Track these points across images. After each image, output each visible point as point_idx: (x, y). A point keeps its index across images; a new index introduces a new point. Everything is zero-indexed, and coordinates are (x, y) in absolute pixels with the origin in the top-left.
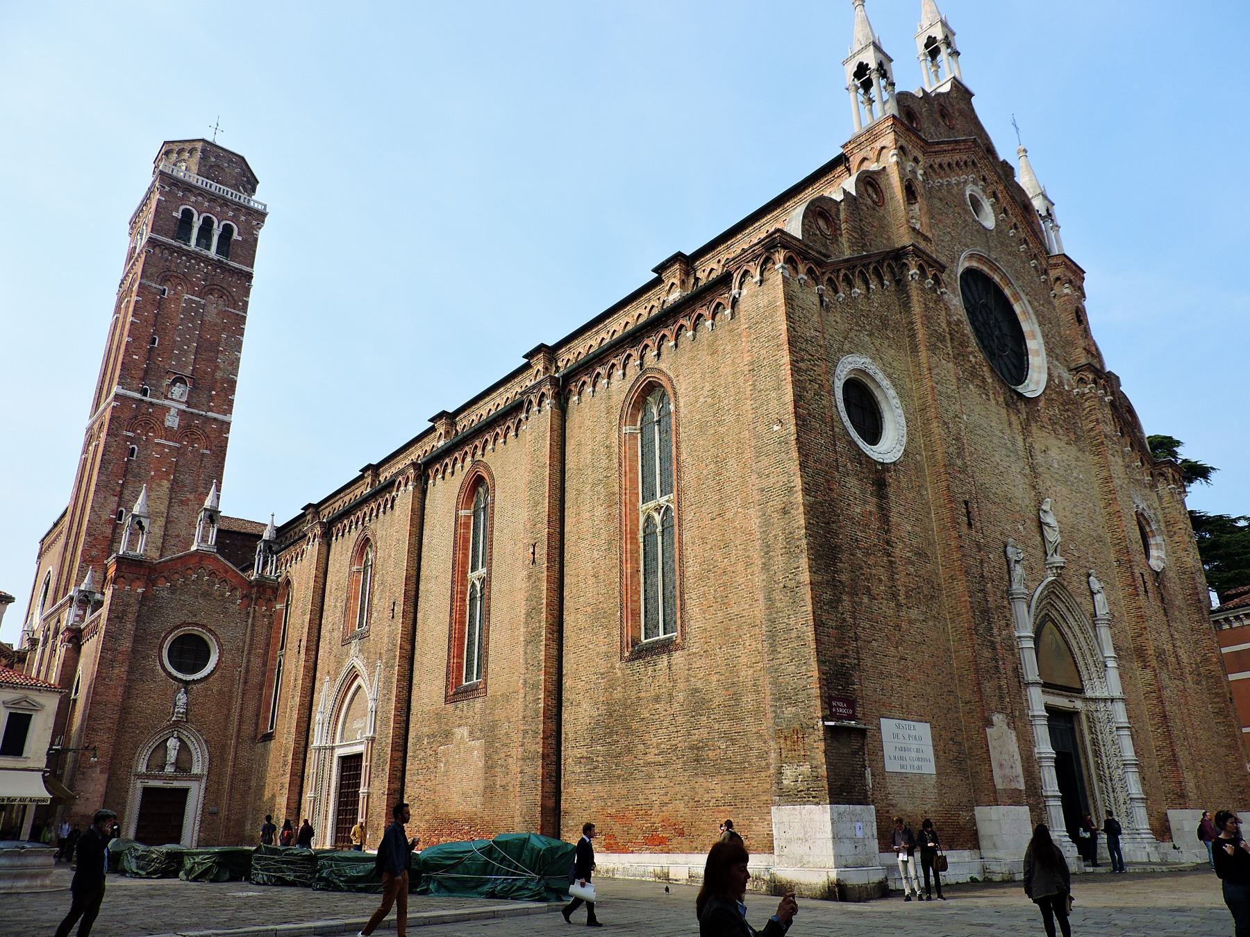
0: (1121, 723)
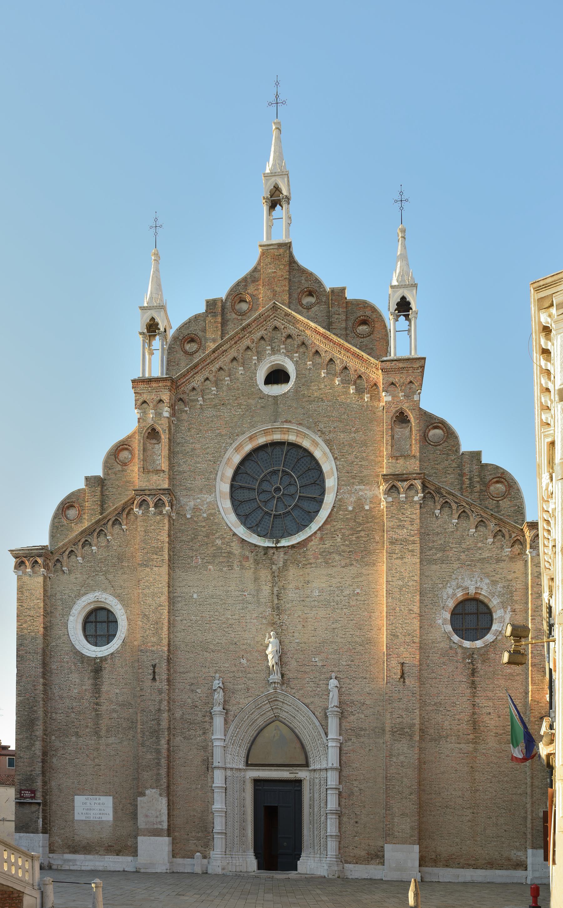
0: (329, 785)
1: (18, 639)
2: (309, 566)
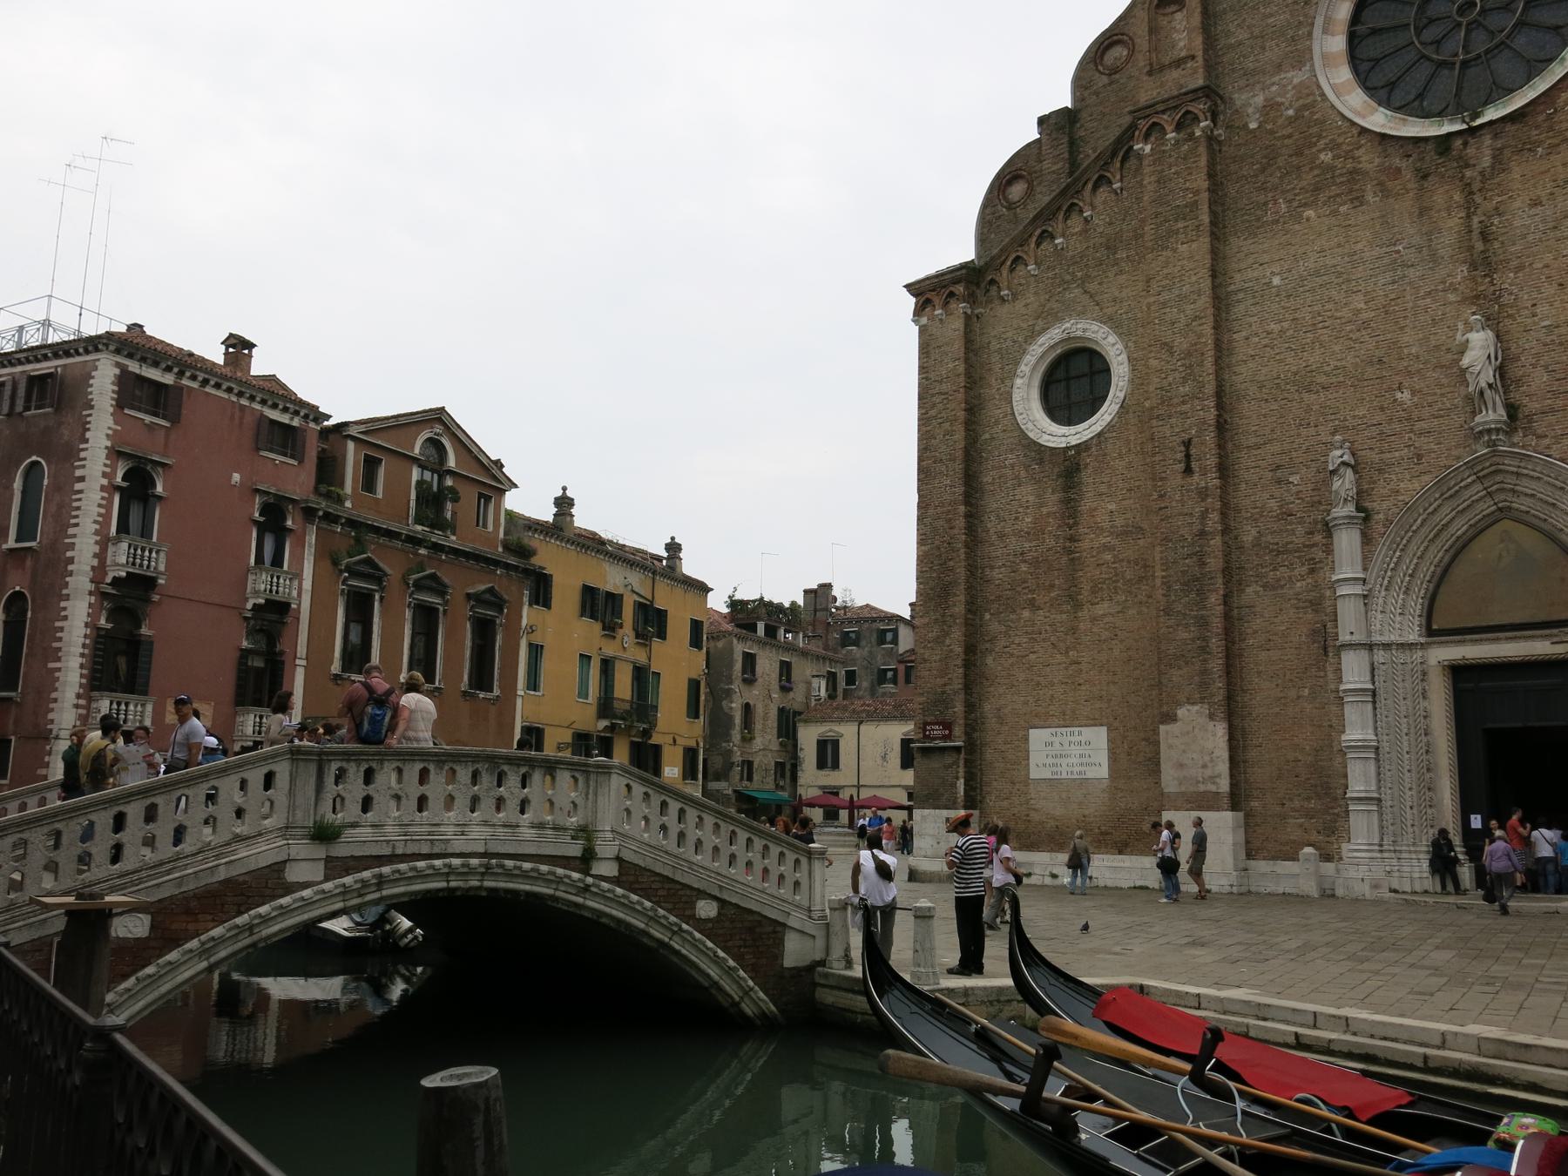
1: (920, 440)
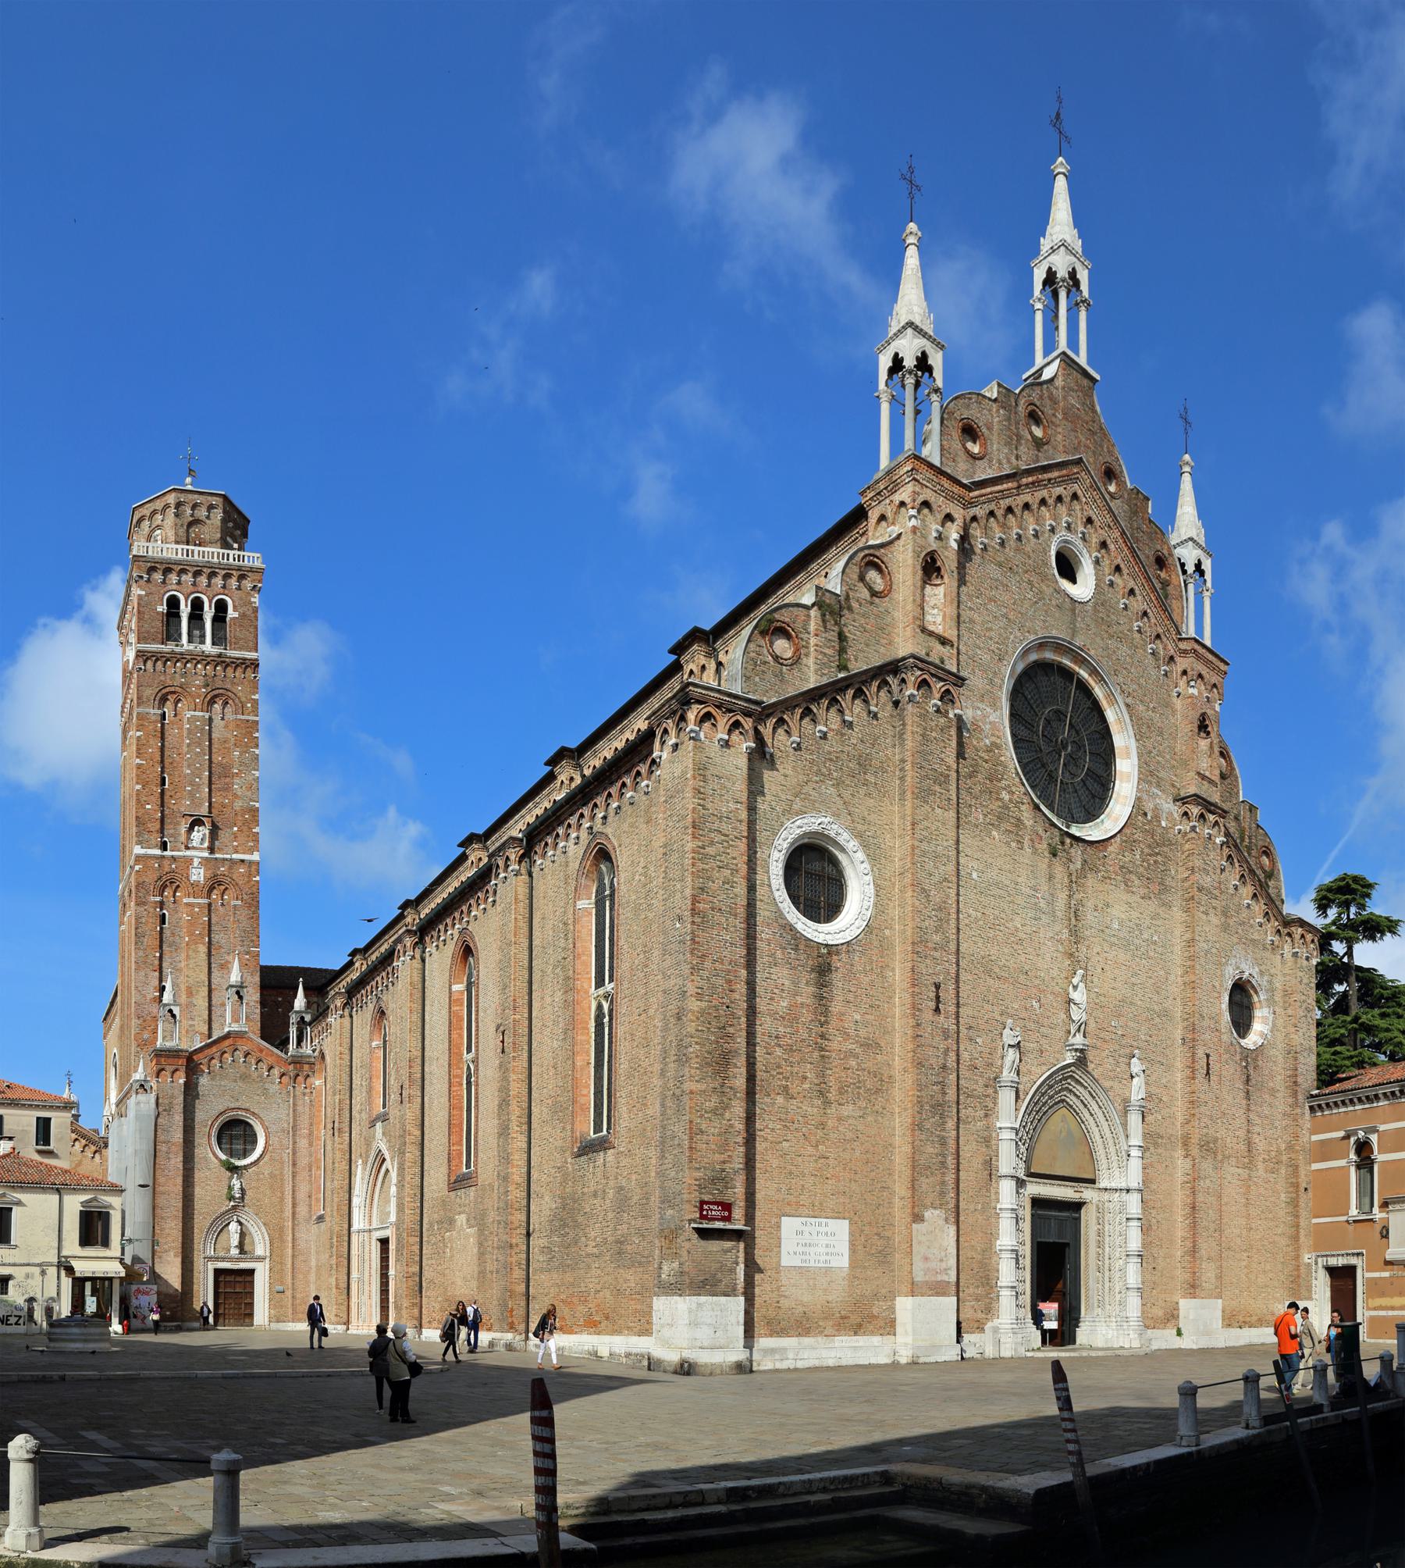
2: (1108, 881)
